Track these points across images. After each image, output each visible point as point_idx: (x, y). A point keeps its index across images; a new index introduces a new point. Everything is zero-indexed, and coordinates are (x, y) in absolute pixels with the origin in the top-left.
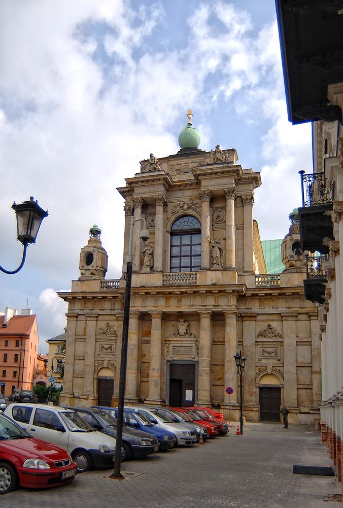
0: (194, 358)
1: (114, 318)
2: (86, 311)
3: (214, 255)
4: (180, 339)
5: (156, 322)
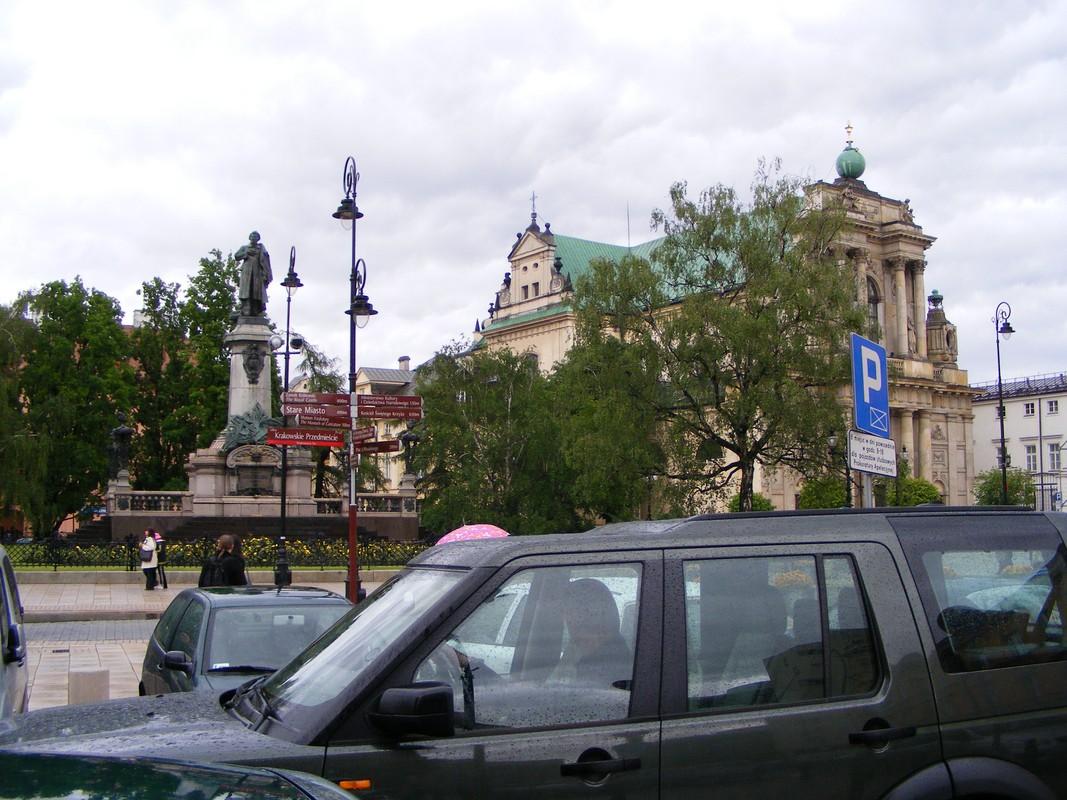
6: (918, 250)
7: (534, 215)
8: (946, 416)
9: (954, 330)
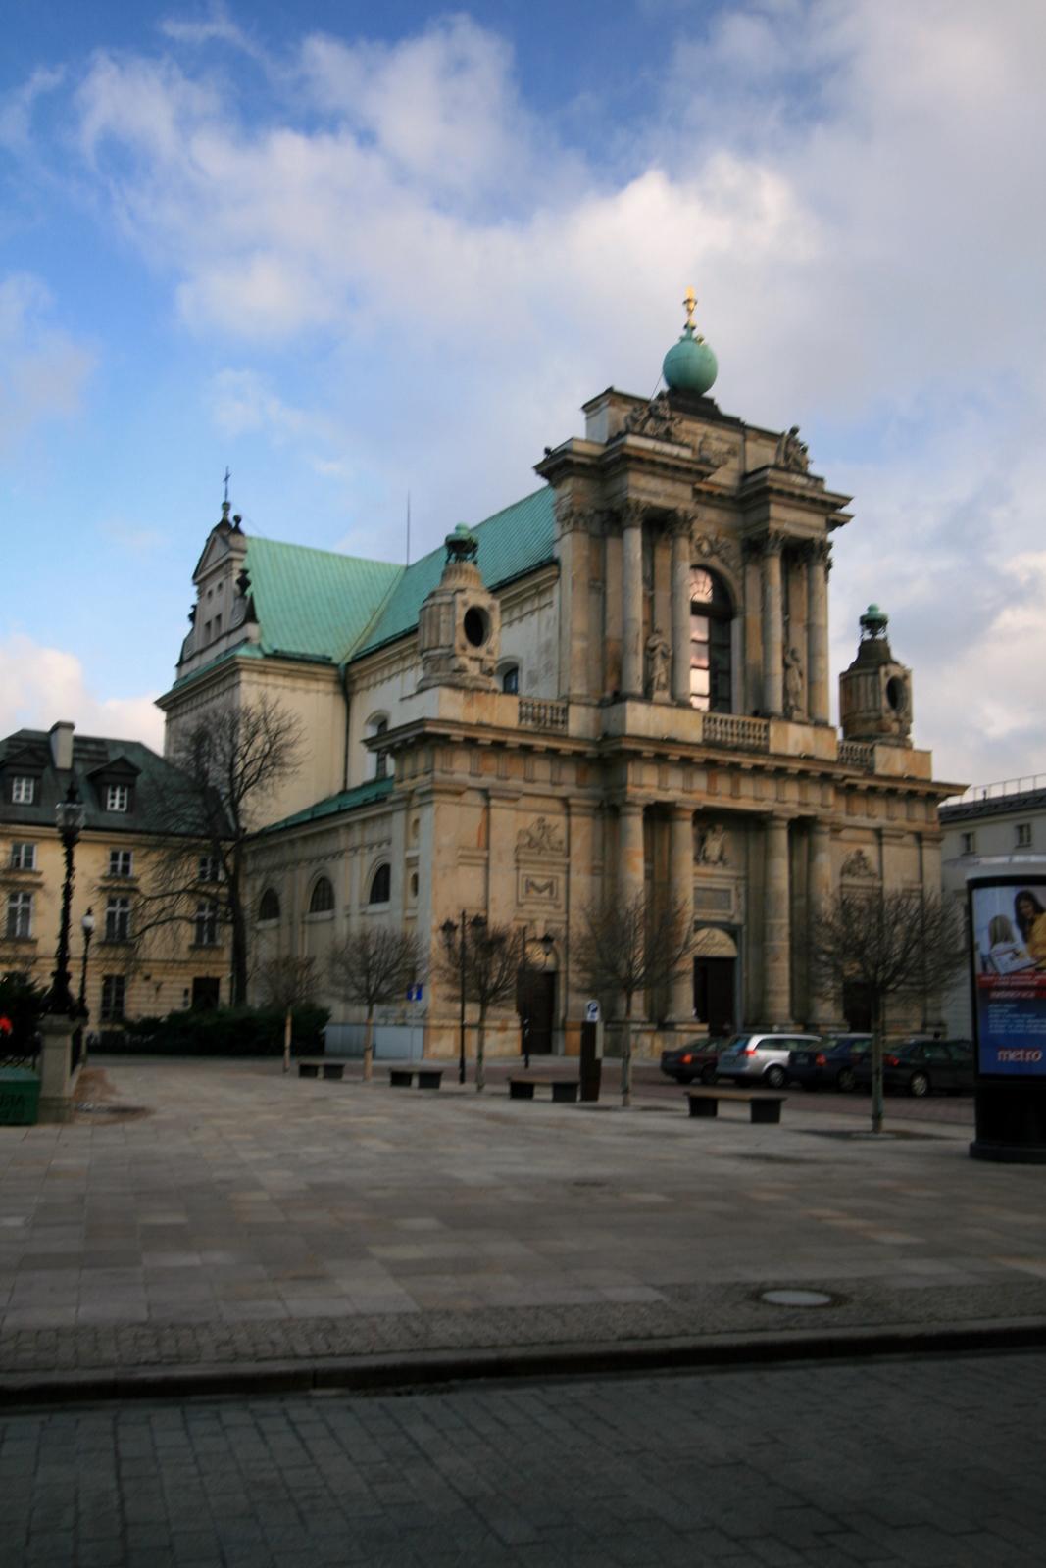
0: (733, 917)
1: (556, 805)
2: (487, 781)
3: (792, 685)
4: (708, 870)
5: (685, 830)
6: (817, 521)
7: (226, 506)
8: (879, 833)
9: (906, 677)
